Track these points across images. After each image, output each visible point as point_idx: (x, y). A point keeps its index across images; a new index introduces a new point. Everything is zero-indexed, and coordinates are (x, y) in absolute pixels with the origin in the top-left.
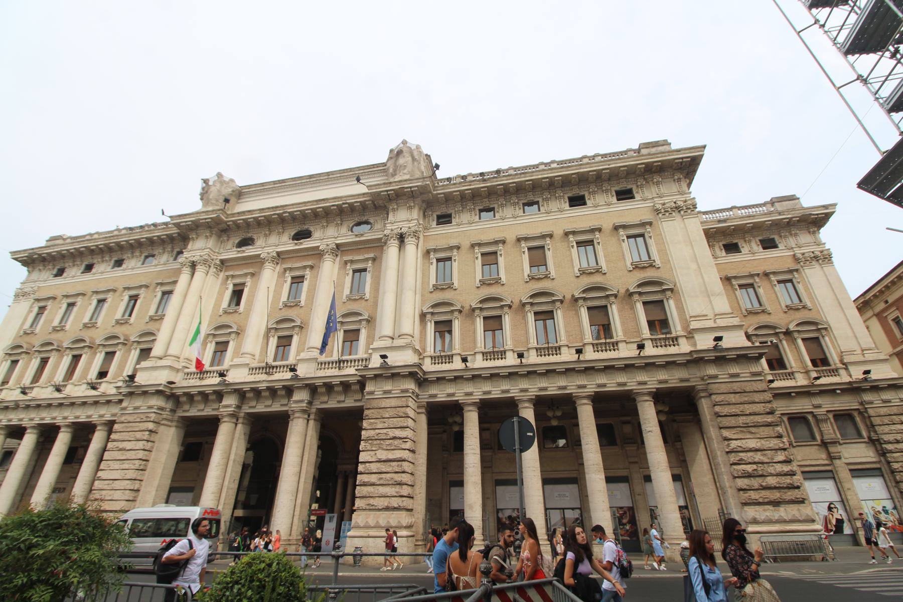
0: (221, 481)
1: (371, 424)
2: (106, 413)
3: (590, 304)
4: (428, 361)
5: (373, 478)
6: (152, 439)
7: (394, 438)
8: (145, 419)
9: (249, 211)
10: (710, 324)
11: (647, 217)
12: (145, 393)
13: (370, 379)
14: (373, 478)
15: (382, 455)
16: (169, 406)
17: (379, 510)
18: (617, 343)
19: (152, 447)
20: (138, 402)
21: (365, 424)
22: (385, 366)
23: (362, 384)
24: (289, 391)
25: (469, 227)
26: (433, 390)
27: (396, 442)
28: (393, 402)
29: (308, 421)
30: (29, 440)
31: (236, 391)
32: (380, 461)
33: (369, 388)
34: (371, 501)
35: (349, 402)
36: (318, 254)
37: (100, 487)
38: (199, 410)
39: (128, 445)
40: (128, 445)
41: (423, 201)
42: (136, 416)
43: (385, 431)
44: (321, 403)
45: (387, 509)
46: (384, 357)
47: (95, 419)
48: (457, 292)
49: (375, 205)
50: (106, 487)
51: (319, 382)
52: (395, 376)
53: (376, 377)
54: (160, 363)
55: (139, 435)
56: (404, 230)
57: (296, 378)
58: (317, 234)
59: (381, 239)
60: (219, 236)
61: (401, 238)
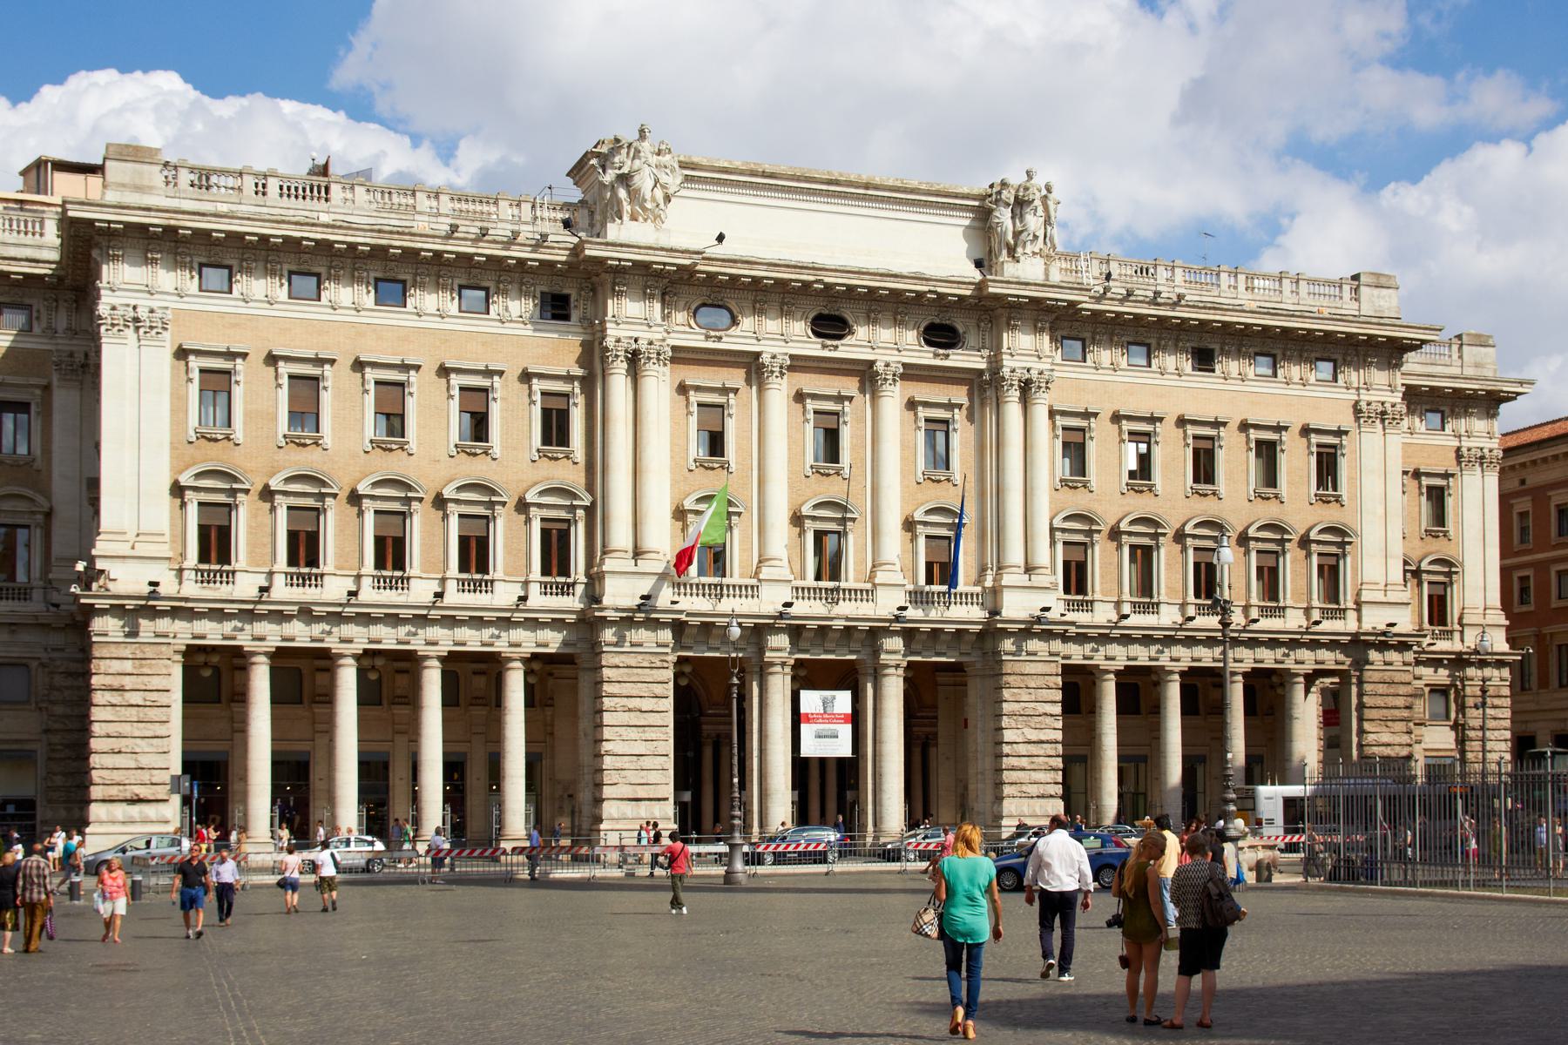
3: (1261, 546)
5: (1024, 762)
8: (659, 664)
10: (1380, 597)
11: (1347, 421)
14: (1024, 762)
15: (1033, 735)
18: (1284, 608)
21: (1006, 694)
27: (1048, 720)
28: (1040, 668)
32: (1029, 742)
36: (866, 375)
39: (647, 704)
40: (647, 704)
42: (640, 657)
45: (1042, 797)
47: (501, 646)
50: (626, 766)
55: (658, 689)
56: (1034, 375)
58: (862, 332)
59: (980, 372)
61: (1026, 387)
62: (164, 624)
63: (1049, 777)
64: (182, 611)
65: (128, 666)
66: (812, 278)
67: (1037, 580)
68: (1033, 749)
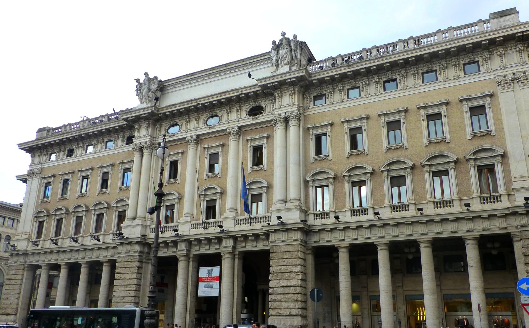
0: (185, 297)
1: (275, 263)
2: (109, 255)
4: (311, 217)
5: (279, 297)
6: (140, 272)
7: (291, 272)
9: (173, 105)
12: (130, 243)
13: (272, 232)
16: (146, 250)
17: (286, 316)
19: (141, 277)
20: (126, 248)
21: (271, 263)
22: (281, 224)
23: (267, 234)
24: (219, 240)
25: (338, 107)
26: (316, 238)
27: (292, 275)
29: (234, 259)
30: (63, 272)
31: (185, 240)
32: (282, 287)
33: (272, 237)
34: (279, 311)
35: (260, 246)
37: (116, 301)
38: (164, 253)
39: (128, 276)
40: (128, 276)
41: (302, 87)
43: (285, 267)
44: (242, 247)
46: (279, 218)
47: (101, 259)
48: (332, 162)
49: (264, 93)
50: (119, 301)
51: (238, 234)
52: (288, 230)
53: (276, 231)
54: (136, 222)
55: (132, 270)
57: (223, 231)
60: (154, 125)
62: (22, 259)
63: (292, 305)
64: (25, 254)
65: (13, 272)
66: (196, 104)
67: (290, 205)
68: (286, 291)
